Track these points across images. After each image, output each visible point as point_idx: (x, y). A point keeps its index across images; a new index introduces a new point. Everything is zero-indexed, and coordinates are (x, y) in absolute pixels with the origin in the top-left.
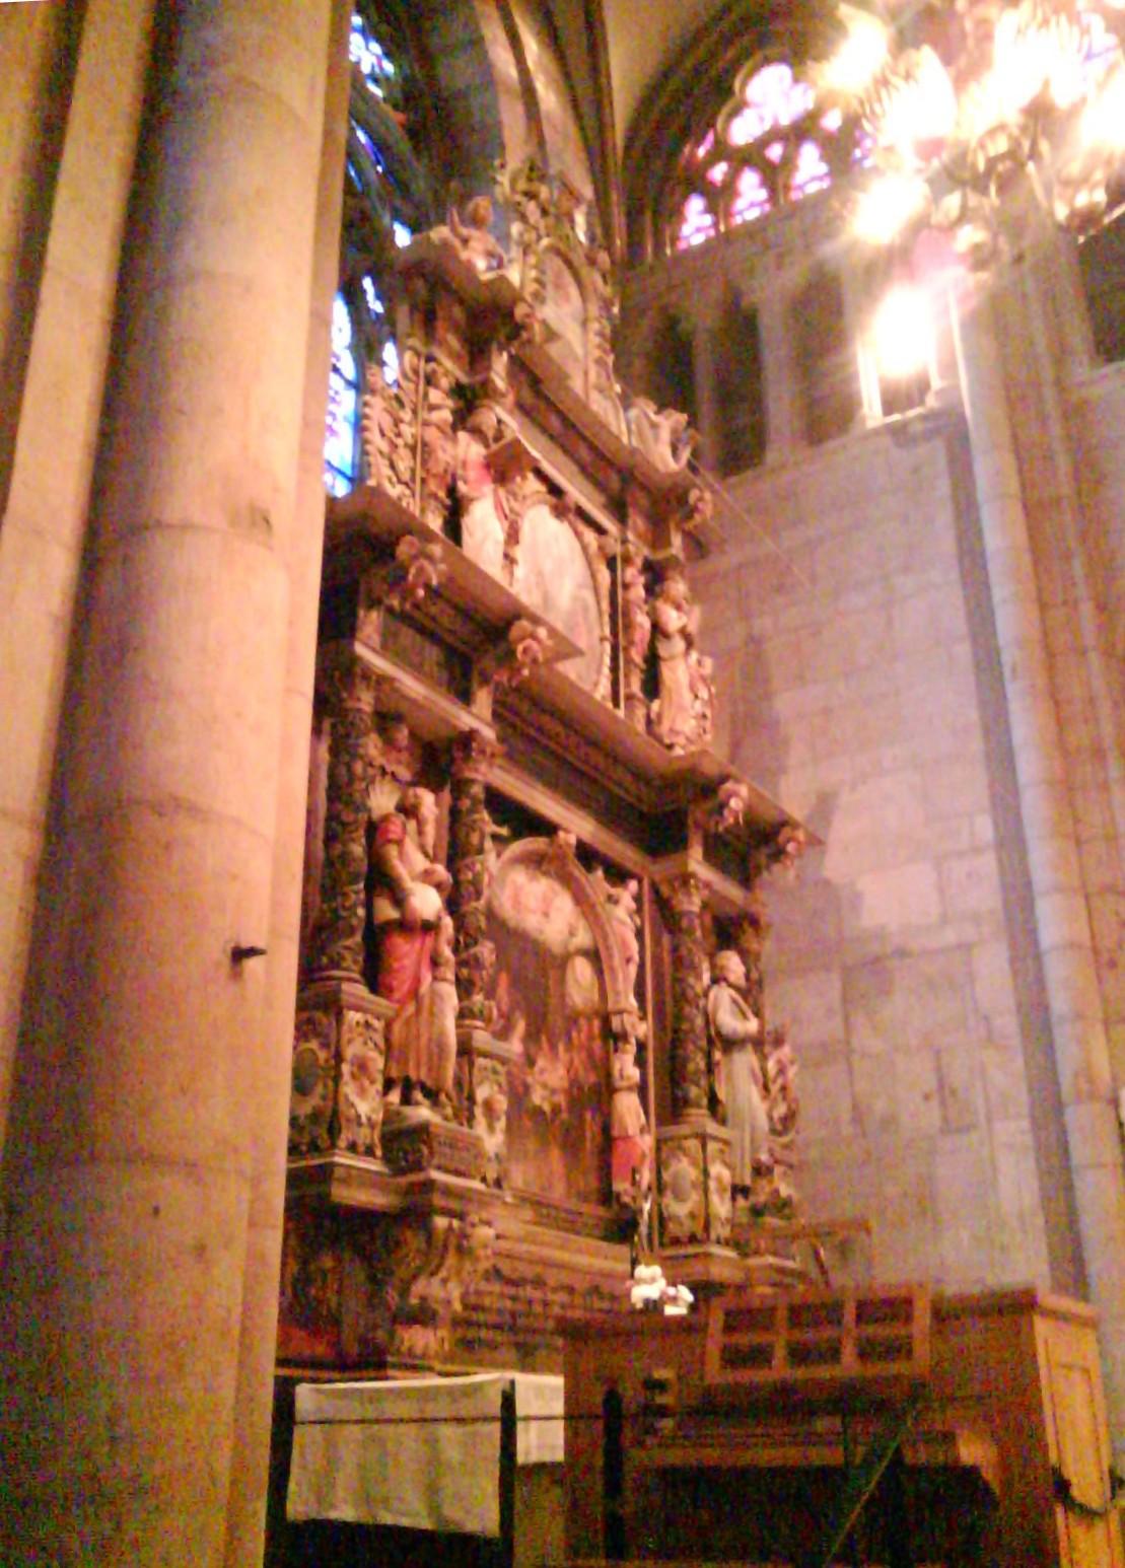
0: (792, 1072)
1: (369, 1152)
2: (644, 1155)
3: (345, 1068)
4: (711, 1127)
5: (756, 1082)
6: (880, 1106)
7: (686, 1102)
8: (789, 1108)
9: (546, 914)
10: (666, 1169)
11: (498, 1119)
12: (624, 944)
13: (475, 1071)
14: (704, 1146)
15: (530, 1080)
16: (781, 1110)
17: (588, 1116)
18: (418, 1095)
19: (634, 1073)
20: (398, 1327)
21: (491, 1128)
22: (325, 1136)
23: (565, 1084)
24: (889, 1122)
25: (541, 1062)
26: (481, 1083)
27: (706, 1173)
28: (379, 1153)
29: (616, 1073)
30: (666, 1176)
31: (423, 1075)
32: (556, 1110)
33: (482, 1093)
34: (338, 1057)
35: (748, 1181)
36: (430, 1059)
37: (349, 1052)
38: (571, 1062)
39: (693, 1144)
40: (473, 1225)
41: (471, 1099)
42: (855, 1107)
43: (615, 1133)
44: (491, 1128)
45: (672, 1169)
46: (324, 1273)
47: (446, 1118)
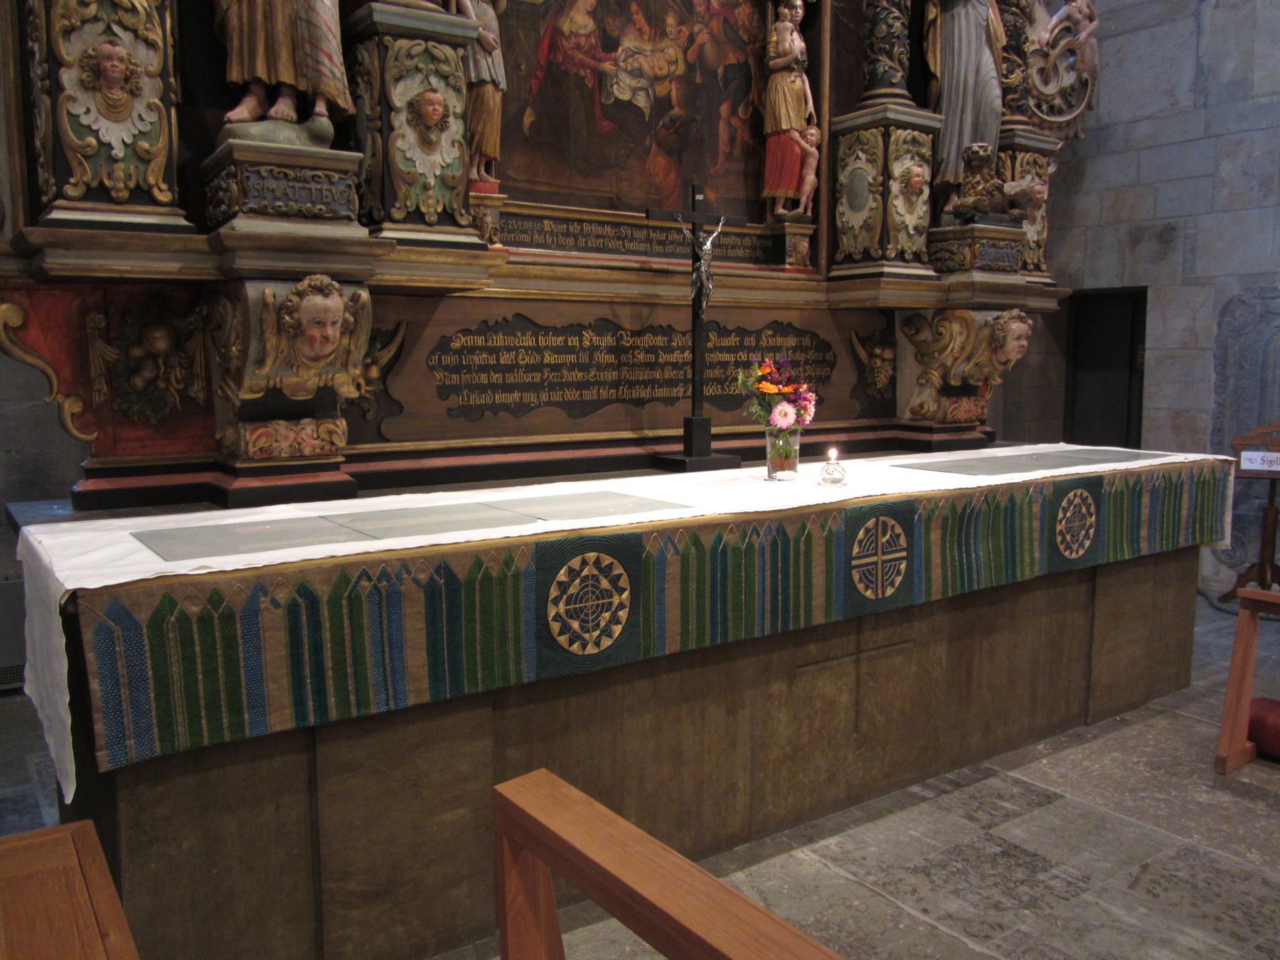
0: (1087, 29)
1: (141, 195)
2: (805, 155)
3: (68, 77)
4: (899, 109)
5: (990, 42)
6: (1229, 68)
7: (874, 80)
8: (1079, 78)
10: (844, 168)
11: (443, 125)
13: (390, 62)
14: (886, 136)
15: (607, 66)
16: (1068, 79)
17: (724, 109)
18: (284, 107)
19: (796, 43)
20: (240, 425)
21: (427, 144)
22: (52, 181)
23: (681, 69)
24: (1241, 86)
25: (629, 43)
26: (398, 79)
27: (887, 173)
28: (165, 197)
29: (772, 51)
30: (843, 178)
31: (286, 76)
32: (661, 105)
33: (400, 95)
34: (55, 62)
35: (961, 180)
36: (295, 47)
37: (70, 50)
38: (691, 39)
39: (874, 136)
40: (301, 295)
41: (386, 106)
42: (1200, 70)
43: (768, 128)
44: (427, 144)
45: (849, 169)
46: (154, 357)
47: (317, 138)
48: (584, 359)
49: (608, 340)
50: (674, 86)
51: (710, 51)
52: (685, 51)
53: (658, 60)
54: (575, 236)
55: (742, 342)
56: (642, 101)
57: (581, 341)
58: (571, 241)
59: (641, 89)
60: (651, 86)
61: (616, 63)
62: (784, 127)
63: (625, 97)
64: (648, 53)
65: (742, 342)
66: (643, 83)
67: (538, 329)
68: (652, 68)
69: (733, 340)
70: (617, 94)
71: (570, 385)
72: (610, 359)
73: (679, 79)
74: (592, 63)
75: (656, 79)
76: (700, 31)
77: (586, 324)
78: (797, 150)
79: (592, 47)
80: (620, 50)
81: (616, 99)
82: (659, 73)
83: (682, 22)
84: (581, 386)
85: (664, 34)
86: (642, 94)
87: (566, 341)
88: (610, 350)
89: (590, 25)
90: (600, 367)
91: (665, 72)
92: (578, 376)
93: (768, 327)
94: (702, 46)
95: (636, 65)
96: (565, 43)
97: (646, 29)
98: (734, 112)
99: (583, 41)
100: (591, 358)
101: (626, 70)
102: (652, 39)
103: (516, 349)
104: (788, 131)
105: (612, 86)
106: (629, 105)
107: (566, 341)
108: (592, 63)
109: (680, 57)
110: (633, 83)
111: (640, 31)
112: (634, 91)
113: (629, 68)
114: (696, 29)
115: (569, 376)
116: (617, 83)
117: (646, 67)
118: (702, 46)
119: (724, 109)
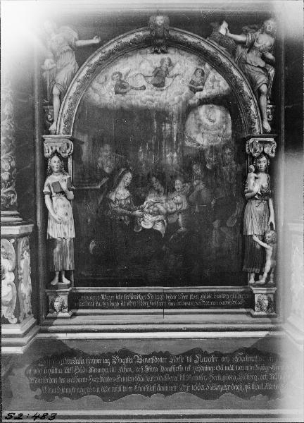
2: (263, 249)
9: (159, 85)
12: (253, 83)
15: (137, 212)
23: (185, 206)
32: (172, 228)
38: (192, 190)
48: (113, 371)
49: (128, 360)
50: (180, 216)
51: (205, 194)
52: (188, 197)
53: (170, 204)
54: (120, 302)
55: (219, 360)
56: (159, 227)
57: (111, 361)
58: (118, 304)
59: (159, 221)
60: (166, 218)
61: (142, 210)
62: (249, 234)
63: (149, 226)
64: (164, 201)
65: (219, 360)
66: (160, 217)
67: (85, 356)
68: (166, 209)
69: (213, 359)
70: (143, 225)
71: (103, 384)
72: (130, 370)
73: (184, 211)
74: (128, 212)
75: (168, 215)
76: (198, 184)
77: (114, 352)
78: (258, 247)
79: (130, 204)
80: (145, 203)
81: (144, 229)
82: (170, 210)
83: (185, 182)
84: (111, 384)
85: (174, 190)
86: (160, 223)
87: (102, 361)
88: (128, 365)
89: (127, 193)
90: (122, 375)
91: (174, 209)
92: (109, 379)
93: (240, 350)
94: (199, 192)
95: (155, 209)
96: (112, 205)
97: (162, 189)
98: (223, 224)
99: (123, 202)
100: (117, 370)
101: (149, 213)
102: (166, 194)
103: (74, 366)
104: (251, 236)
105: (140, 222)
106: (152, 231)
107: (102, 361)
108: (128, 212)
109: (184, 199)
110: (154, 219)
111: (158, 192)
112: (154, 223)
113: (151, 211)
114: (195, 183)
115: (102, 379)
116: (143, 220)
117: (162, 209)
118: (199, 192)
119: (216, 224)
